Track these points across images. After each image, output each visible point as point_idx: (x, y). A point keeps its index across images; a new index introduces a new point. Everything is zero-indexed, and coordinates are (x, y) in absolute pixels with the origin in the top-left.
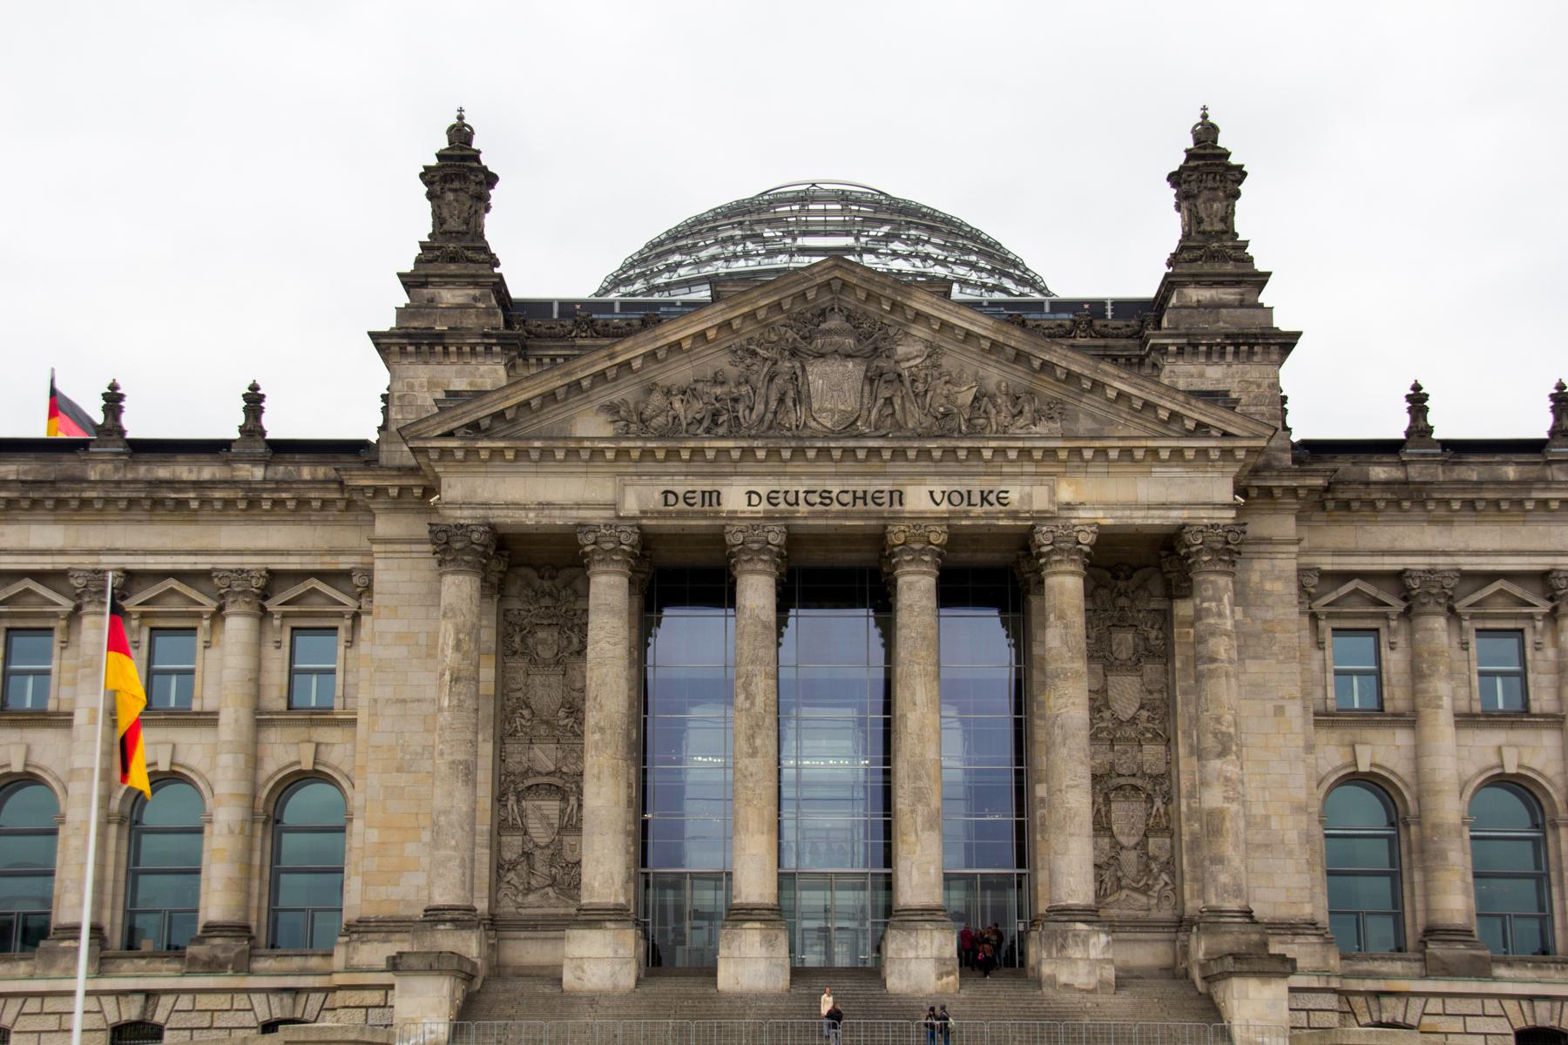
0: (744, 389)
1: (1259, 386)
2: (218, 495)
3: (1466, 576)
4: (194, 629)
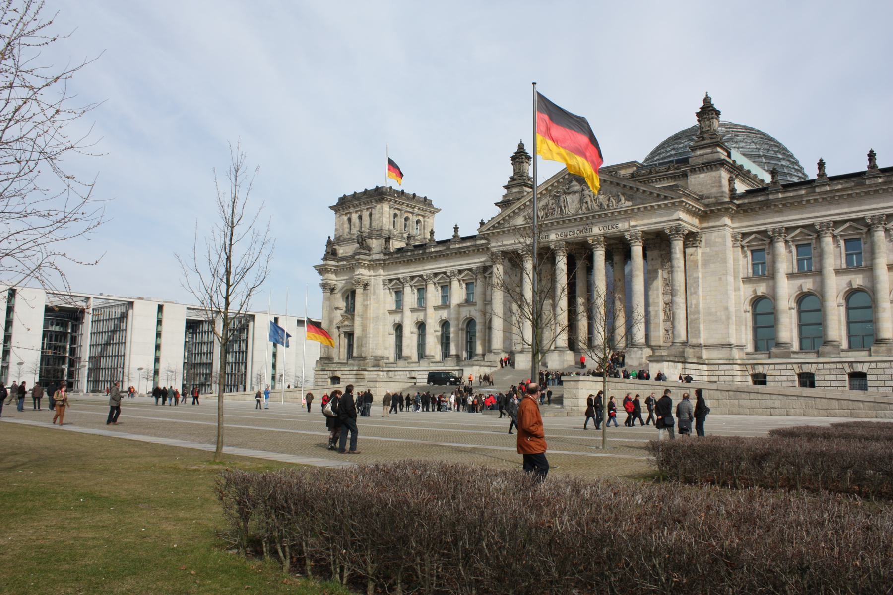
0: (554, 205)
1: (715, 177)
2: (471, 249)
3: (787, 228)
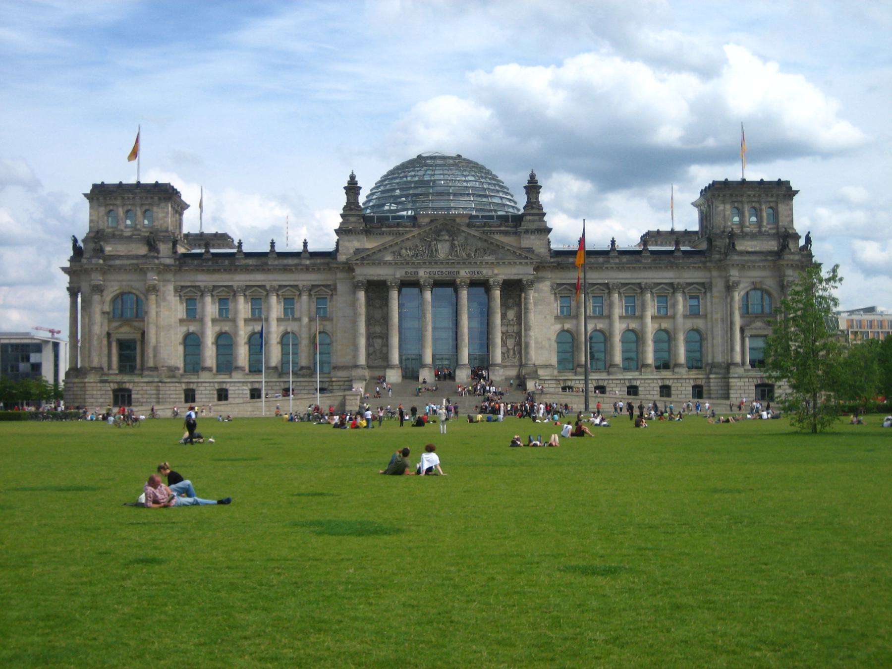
4: (293, 298)
